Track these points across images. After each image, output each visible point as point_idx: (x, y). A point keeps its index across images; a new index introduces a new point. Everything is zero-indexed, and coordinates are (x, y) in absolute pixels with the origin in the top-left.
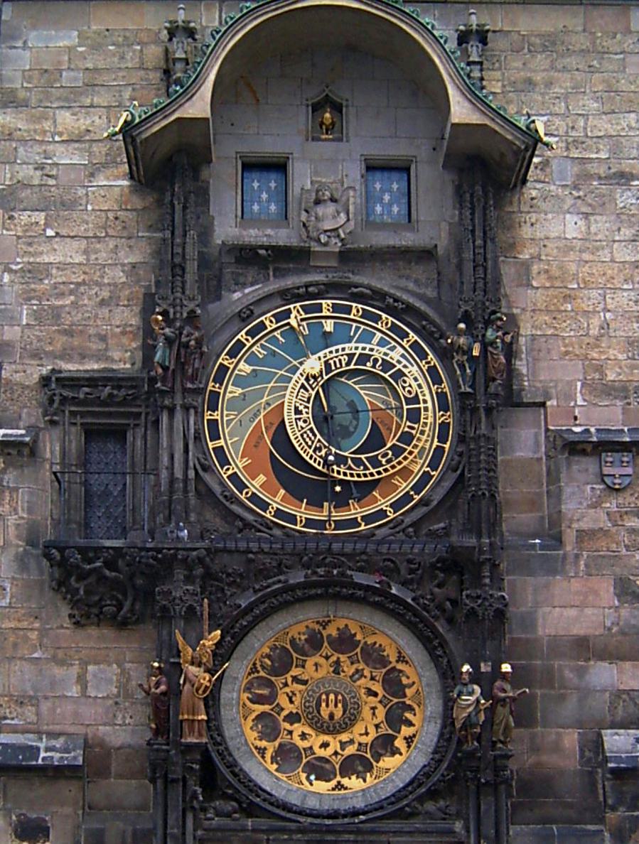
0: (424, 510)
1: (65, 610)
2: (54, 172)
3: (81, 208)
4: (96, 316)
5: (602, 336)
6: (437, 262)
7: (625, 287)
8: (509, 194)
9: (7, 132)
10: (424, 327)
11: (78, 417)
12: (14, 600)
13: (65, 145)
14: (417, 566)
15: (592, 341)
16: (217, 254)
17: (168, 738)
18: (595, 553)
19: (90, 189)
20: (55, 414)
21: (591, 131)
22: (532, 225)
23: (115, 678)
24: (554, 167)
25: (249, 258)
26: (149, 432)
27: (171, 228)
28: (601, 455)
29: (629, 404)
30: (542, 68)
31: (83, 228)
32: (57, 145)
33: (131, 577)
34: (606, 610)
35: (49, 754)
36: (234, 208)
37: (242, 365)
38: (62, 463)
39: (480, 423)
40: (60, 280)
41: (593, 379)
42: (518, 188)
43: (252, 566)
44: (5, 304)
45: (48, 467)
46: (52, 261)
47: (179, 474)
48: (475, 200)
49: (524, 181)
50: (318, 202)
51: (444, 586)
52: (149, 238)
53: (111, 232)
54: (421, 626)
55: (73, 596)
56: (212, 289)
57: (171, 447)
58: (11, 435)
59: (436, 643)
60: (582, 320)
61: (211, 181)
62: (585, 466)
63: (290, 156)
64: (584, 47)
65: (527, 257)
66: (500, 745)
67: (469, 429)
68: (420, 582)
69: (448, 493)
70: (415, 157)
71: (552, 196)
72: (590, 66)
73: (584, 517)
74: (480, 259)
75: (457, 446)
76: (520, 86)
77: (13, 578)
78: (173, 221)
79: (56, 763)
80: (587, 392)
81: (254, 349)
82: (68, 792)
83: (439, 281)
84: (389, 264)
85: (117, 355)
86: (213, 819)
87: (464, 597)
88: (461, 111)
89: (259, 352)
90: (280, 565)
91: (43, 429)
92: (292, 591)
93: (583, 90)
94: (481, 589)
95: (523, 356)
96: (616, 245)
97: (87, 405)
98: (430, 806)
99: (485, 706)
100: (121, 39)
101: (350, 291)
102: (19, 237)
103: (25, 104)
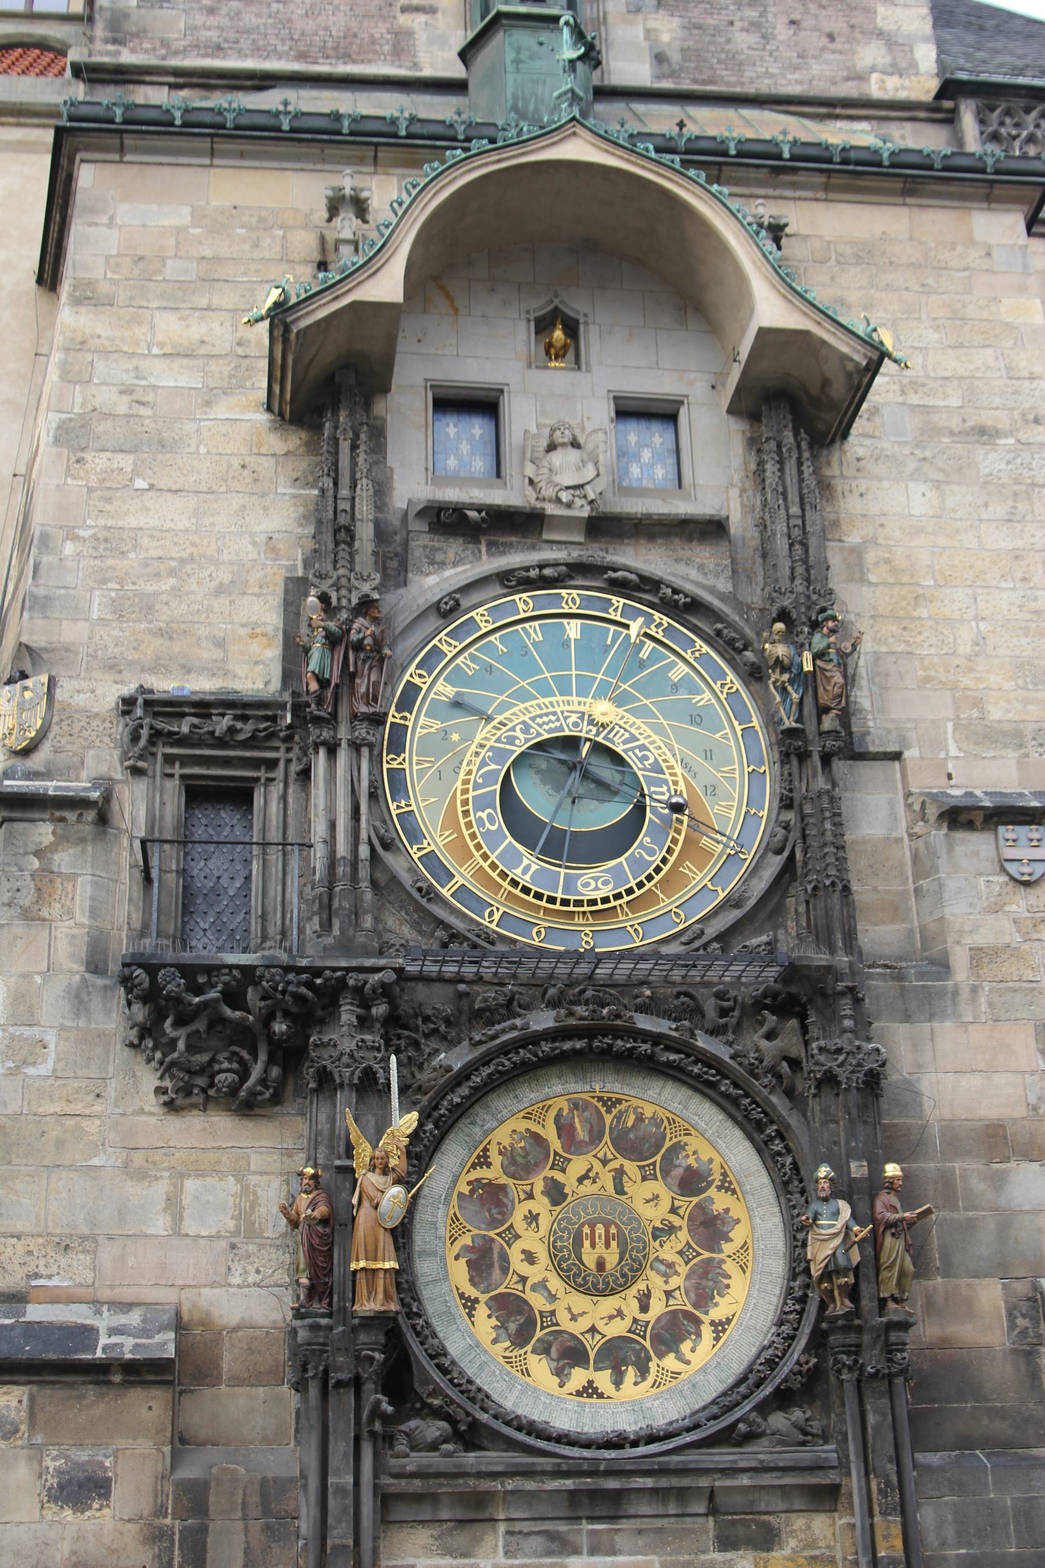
0: (735, 914)
1: (149, 1080)
4: (210, 609)
5: (977, 655)
7: (1003, 585)
8: (825, 452)
9: (79, 339)
10: (719, 633)
11: (177, 765)
12: (62, 1064)
13: (168, 361)
14: (731, 1003)
17: (330, 1304)
18: (1001, 985)
20: (141, 757)
21: (934, 370)
22: (861, 495)
23: (231, 1201)
25: (449, 521)
26: (290, 791)
27: (332, 474)
28: (996, 831)
29: (1027, 756)
30: (858, 285)
31: (191, 480)
33: (268, 1019)
34: (1027, 1076)
35: (115, 1339)
37: (439, 686)
39: (815, 776)
40: (153, 553)
41: (970, 718)
43: (465, 1002)
44: (64, 587)
45: (125, 842)
46: (142, 524)
47: (342, 849)
48: (784, 450)
49: (845, 435)
50: (552, 447)
51: (776, 1038)
52: (295, 496)
54: (746, 1101)
55: (165, 1055)
56: (390, 572)
57: (331, 809)
58: (67, 788)
59: (771, 1130)
61: (389, 418)
62: (976, 847)
63: (506, 389)
66: (892, 1305)
67: (797, 783)
68: (738, 1029)
69: (771, 887)
70: (687, 396)
72: (923, 285)
73: (979, 926)
75: (779, 814)
77: (62, 1028)
78: (336, 463)
79: (128, 1356)
81: (458, 661)
82: (145, 1410)
84: (660, 541)
86: (407, 1456)
87: (816, 1051)
88: (770, 310)
89: (468, 666)
90: (511, 1000)
91: (119, 782)
92: (534, 1044)
94: (840, 1037)
95: (864, 683)
96: (984, 527)
97: (192, 746)
98: (778, 1420)
99: (861, 1235)
100: (254, 221)
102: (91, 490)
103: (109, 302)
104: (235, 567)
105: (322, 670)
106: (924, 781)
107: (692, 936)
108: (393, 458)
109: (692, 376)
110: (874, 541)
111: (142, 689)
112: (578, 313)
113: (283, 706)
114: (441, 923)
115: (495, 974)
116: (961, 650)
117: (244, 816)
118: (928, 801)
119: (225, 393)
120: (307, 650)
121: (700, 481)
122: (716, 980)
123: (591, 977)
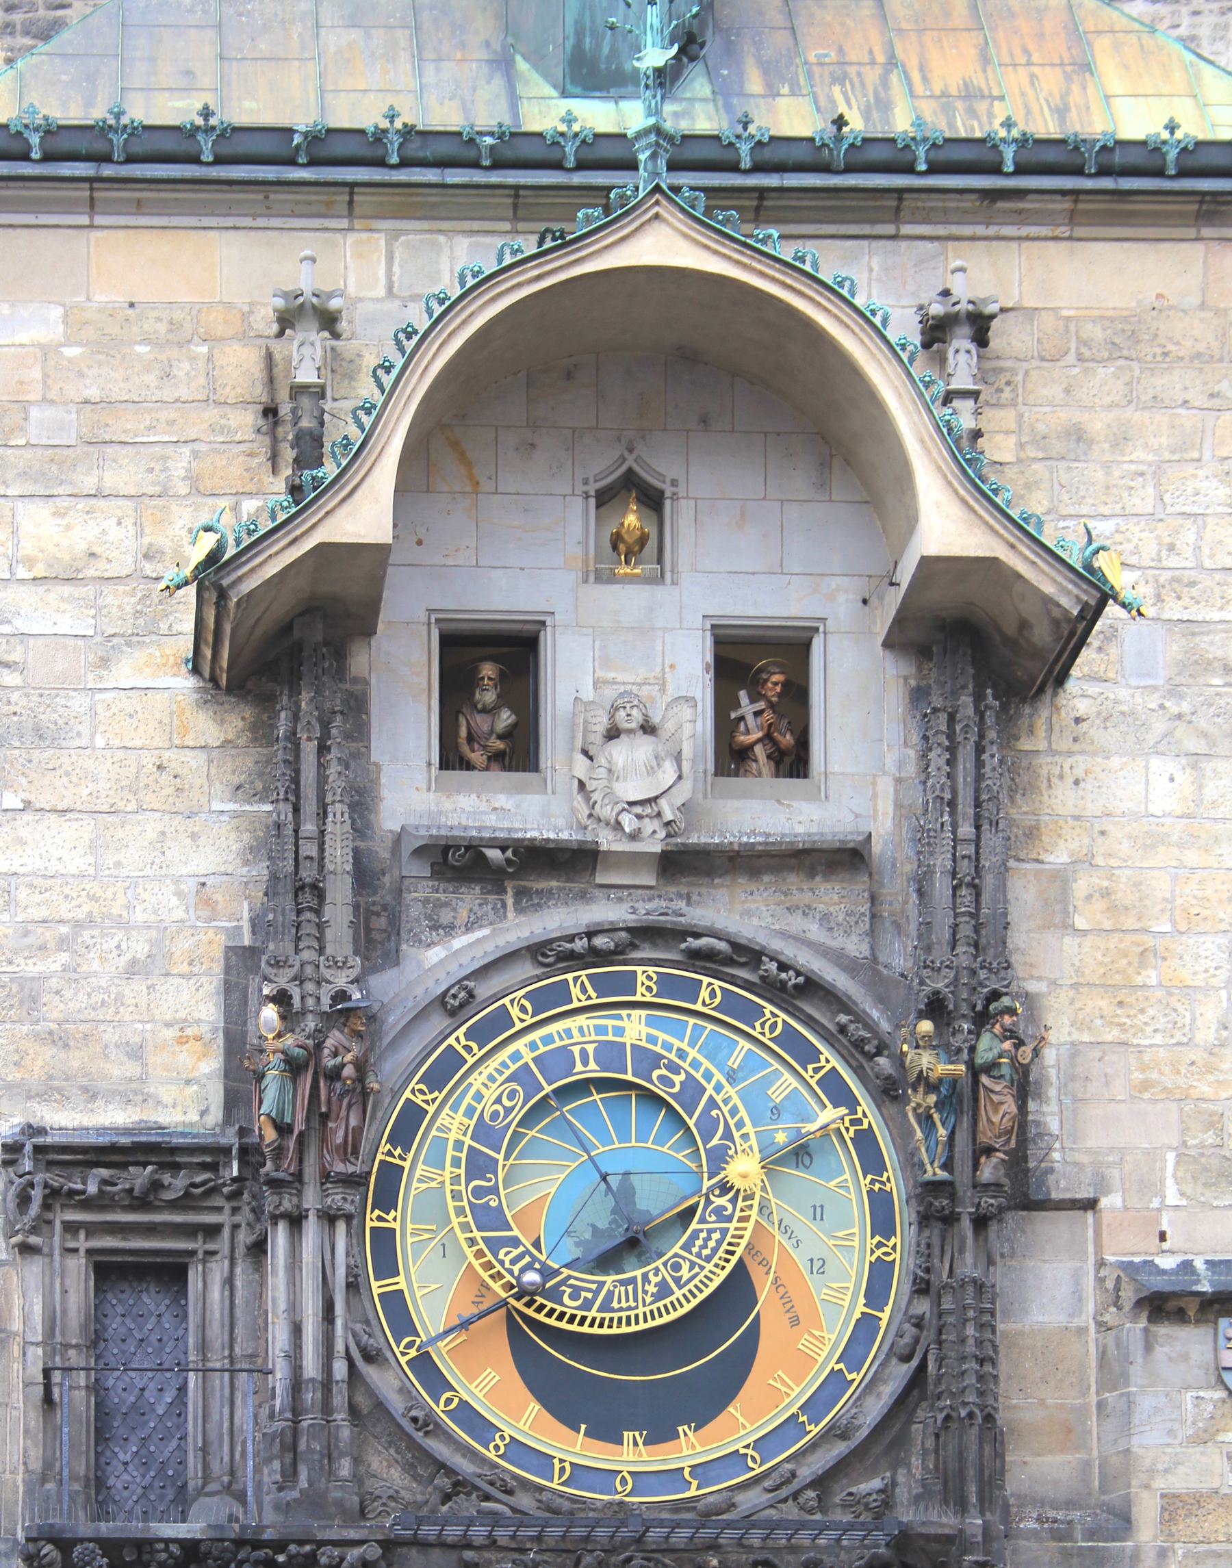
0: (840, 1448)
2: (17, 656)
3: (78, 743)
6: (871, 875)
8: (1027, 710)
10: (842, 1029)
15: (1198, 1055)
16: (385, 855)
19: (98, 696)
21: (1212, 556)
22: (1077, 782)
24: (1126, 645)
25: (462, 863)
27: (292, 798)
28: (1216, 1323)
32: (22, 588)
36: (424, 743)
38: (48, 1341)
39: (962, 1251)
41: (1202, 1146)
42: (1049, 691)
47: (311, 1367)
49: (1061, 679)
52: (237, 815)
53: (150, 800)
56: (376, 936)
57: (294, 1307)
60: (1181, 1009)
61: (373, 681)
62: (1187, 1344)
64: (1201, 347)
65: (1065, 859)
67: (936, 1261)
69: (890, 1410)
71: (1123, 713)
72: (1212, 395)
73: (1177, 1463)
74: (965, 867)
75: (910, 1302)
76: (1058, 447)
78: (296, 781)
80: (1189, 1175)
83: (873, 916)
84: (766, 878)
85: (167, 1093)
93: (1196, 455)
101: (683, 946)
104: (154, 933)
105: (281, 1112)
106: (1127, 1245)
107: (780, 1483)
108: (379, 750)
109: (834, 582)
110: (1086, 860)
111: (33, 1130)
112: (662, 478)
113: (227, 1151)
114: (441, 1467)
115: (513, 1537)
116: (1200, 1037)
117: (175, 1300)
118: (1125, 1279)
119: (129, 644)
120: (260, 1077)
121: (835, 767)
122: (807, 1543)
123: (639, 1541)
